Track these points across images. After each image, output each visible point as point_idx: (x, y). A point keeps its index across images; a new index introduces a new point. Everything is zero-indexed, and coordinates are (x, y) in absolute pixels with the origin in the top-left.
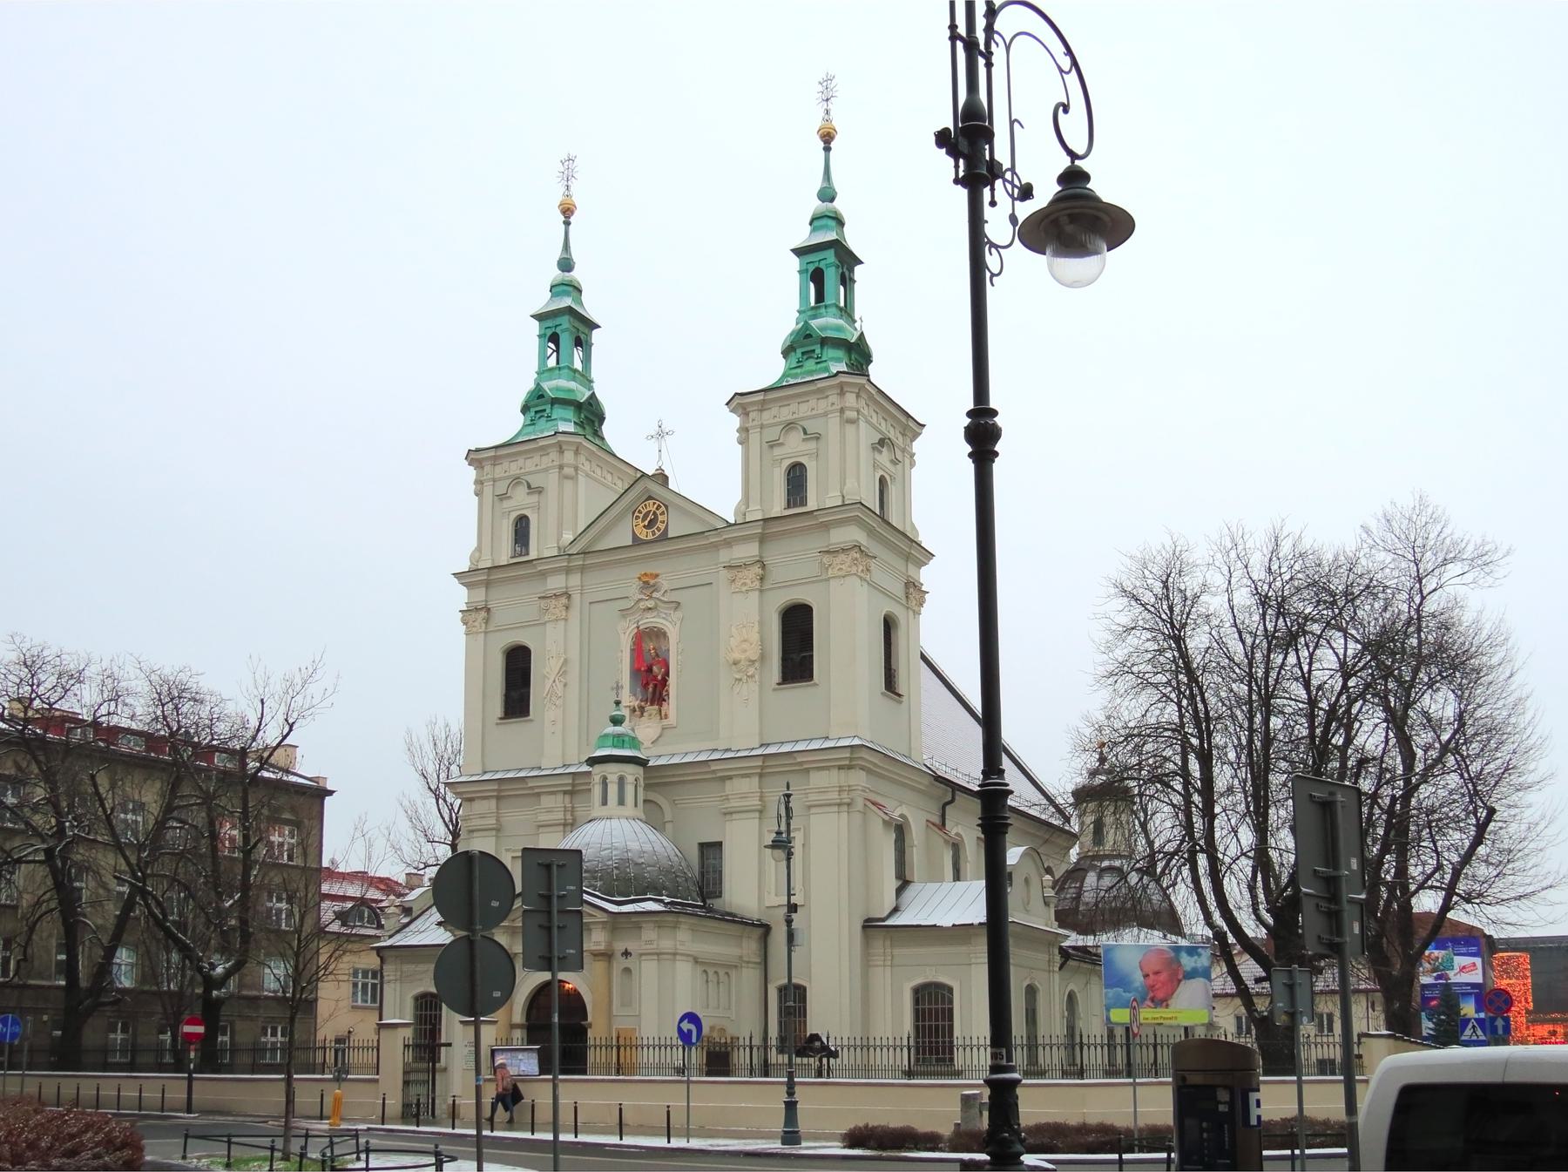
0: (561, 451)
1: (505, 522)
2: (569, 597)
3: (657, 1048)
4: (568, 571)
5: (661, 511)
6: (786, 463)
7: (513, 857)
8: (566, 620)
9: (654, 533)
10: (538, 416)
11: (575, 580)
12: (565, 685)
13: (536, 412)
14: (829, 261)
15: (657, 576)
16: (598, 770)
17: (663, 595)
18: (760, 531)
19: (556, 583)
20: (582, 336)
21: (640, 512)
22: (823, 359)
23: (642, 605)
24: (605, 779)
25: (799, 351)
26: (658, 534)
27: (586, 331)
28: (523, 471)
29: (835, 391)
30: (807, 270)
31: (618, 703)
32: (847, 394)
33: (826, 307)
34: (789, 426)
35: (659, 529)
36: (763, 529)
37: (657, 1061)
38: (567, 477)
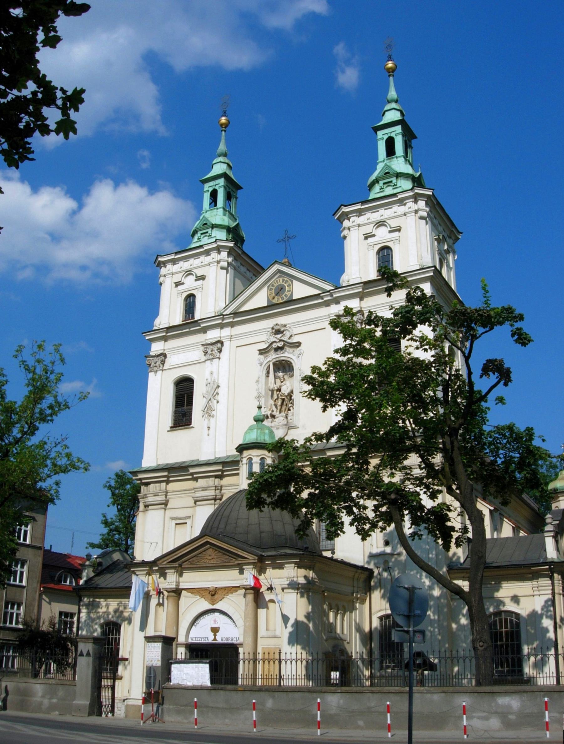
0: (219, 253)
1: (180, 299)
2: (222, 343)
3: (294, 662)
4: (222, 326)
5: (287, 284)
6: (377, 247)
7: (176, 524)
8: (219, 358)
9: (283, 298)
10: (202, 236)
11: (227, 331)
12: (218, 402)
13: (202, 234)
14: (397, 132)
15: (285, 326)
16: (246, 453)
17: (289, 338)
18: (361, 290)
19: (213, 335)
20: (232, 193)
21: (273, 286)
22: (398, 186)
23: (274, 346)
24: (250, 459)
25: (381, 183)
26: (285, 299)
27: (234, 190)
28: (192, 267)
29: (411, 200)
30: (383, 138)
31: (260, 408)
32: (420, 201)
33: (397, 157)
34: (380, 224)
35: (286, 296)
36: (364, 289)
37: (294, 672)
38: (222, 268)
